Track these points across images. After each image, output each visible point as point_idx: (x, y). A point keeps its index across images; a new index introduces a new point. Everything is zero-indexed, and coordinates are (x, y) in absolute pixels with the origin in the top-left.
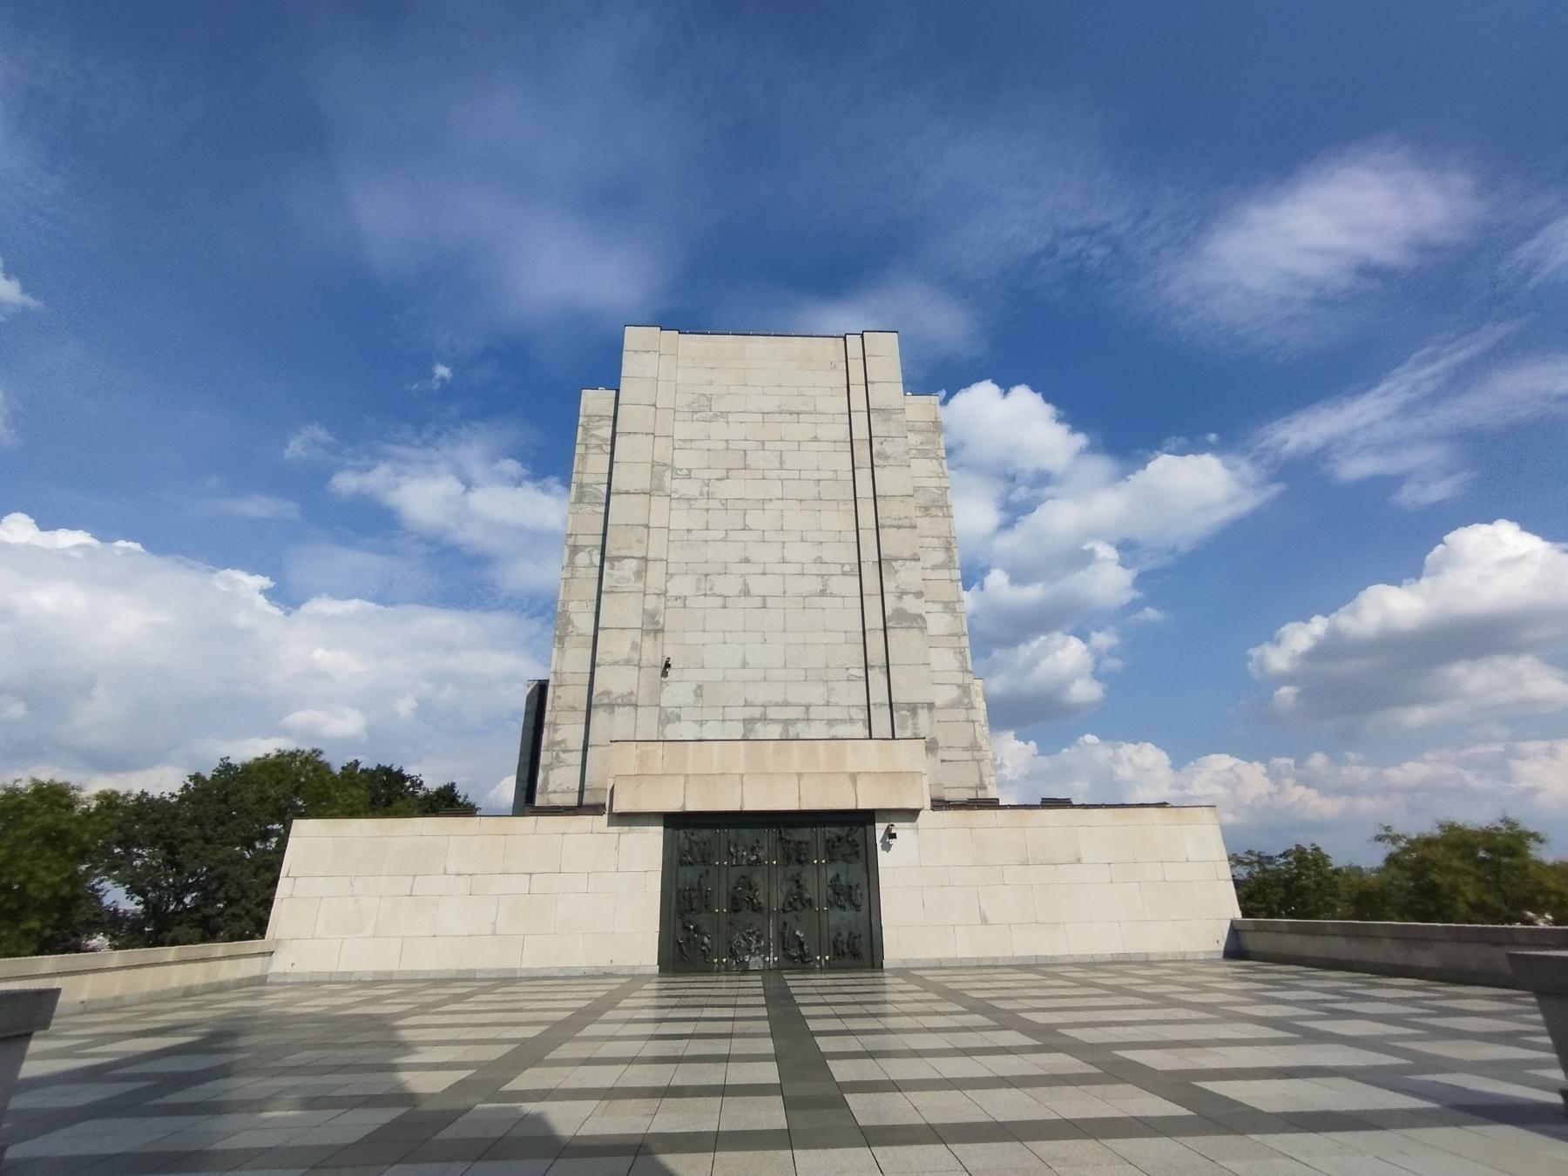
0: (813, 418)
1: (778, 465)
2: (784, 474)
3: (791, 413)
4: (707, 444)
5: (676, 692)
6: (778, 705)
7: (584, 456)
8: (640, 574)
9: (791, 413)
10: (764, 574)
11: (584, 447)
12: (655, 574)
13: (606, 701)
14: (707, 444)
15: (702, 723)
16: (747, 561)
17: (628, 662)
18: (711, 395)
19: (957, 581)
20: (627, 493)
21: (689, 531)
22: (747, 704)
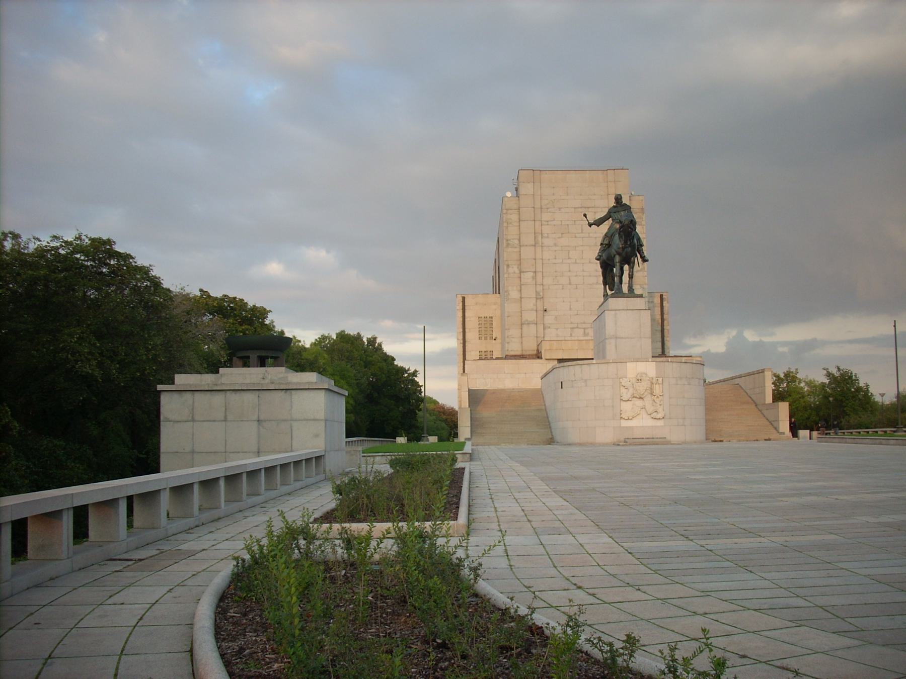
0: (593, 210)
1: (580, 232)
2: (582, 235)
3: (585, 208)
4: (554, 223)
5: (549, 319)
6: (581, 323)
7: (507, 227)
8: (534, 278)
9: (585, 208)
10: (576, 276)
11: (506, 223)
12: (539, 275)
13: (526, 323)
14: (554, 223)
15: (557, 329)
16: (570, 271)
17: (532, 310)
18: (554, 200)
19: (646, 276)
20: (526, 246)
21: (549, 259)
22: (571, 323)
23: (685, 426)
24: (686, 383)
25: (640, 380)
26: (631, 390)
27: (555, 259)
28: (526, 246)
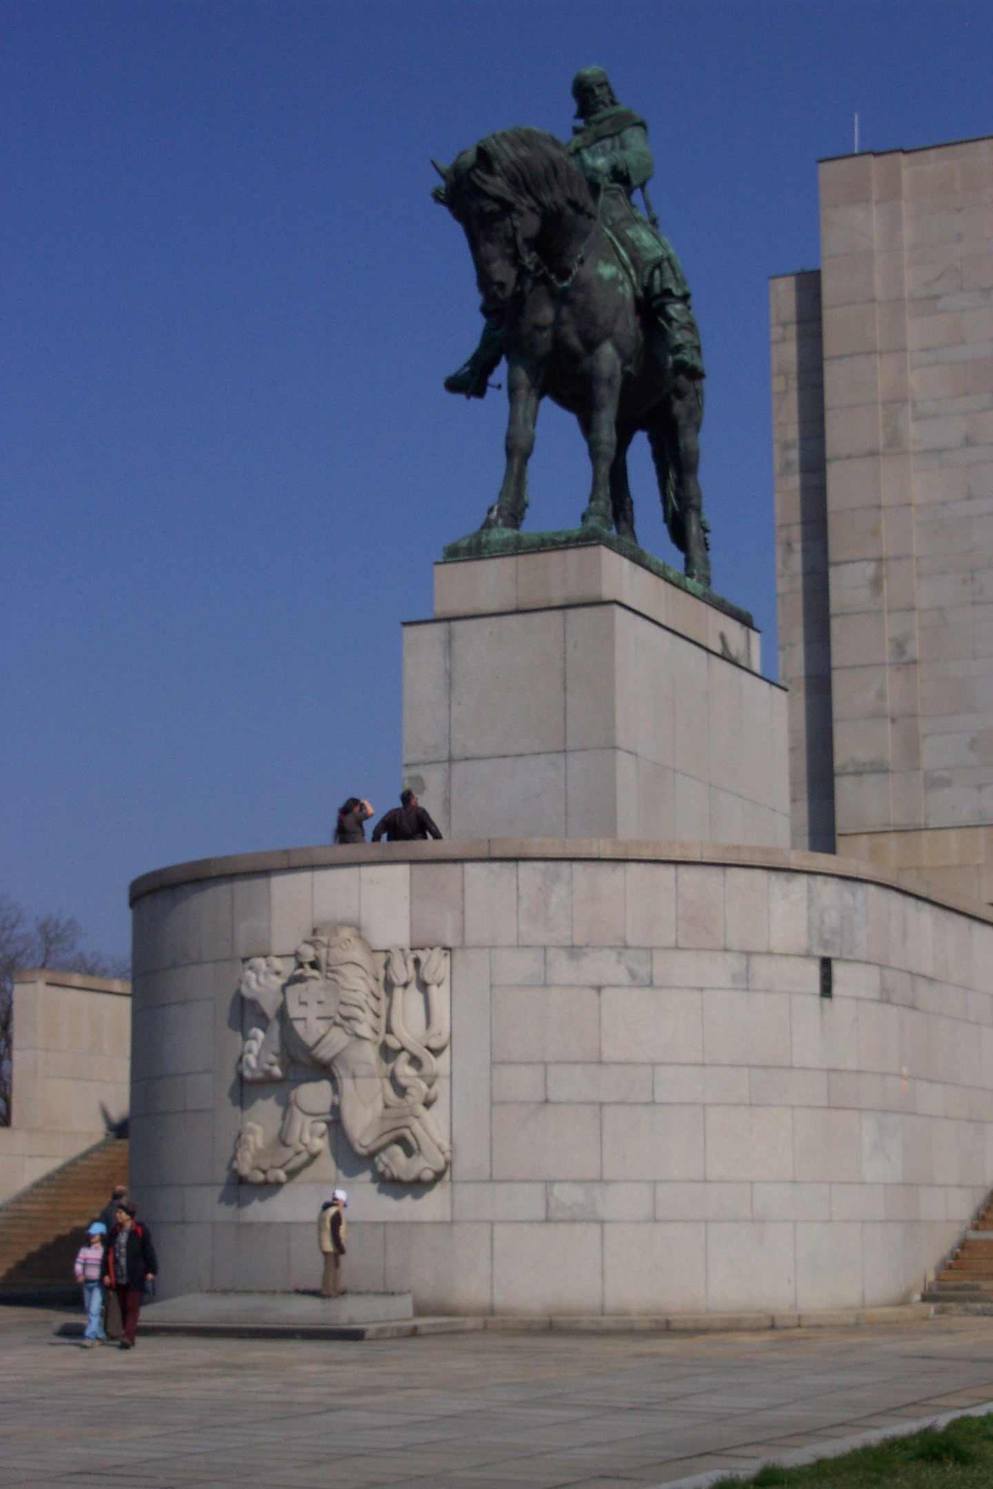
8: (876, 584)
13: (851, 769)
15: (980, 788)
20: (849, 457)
23: (602, 1222)
24: (622, 976)
25: (314, 965)
26: (275, 1027)
27: (970, 497)
28: (849, 457)
